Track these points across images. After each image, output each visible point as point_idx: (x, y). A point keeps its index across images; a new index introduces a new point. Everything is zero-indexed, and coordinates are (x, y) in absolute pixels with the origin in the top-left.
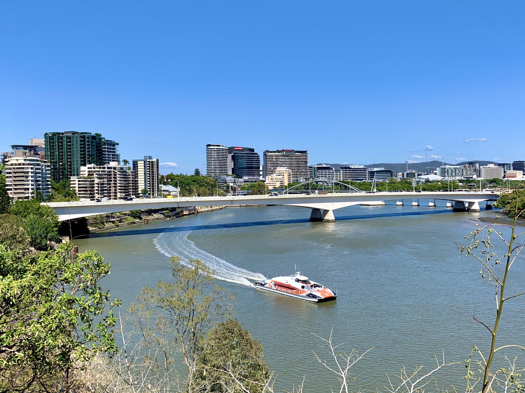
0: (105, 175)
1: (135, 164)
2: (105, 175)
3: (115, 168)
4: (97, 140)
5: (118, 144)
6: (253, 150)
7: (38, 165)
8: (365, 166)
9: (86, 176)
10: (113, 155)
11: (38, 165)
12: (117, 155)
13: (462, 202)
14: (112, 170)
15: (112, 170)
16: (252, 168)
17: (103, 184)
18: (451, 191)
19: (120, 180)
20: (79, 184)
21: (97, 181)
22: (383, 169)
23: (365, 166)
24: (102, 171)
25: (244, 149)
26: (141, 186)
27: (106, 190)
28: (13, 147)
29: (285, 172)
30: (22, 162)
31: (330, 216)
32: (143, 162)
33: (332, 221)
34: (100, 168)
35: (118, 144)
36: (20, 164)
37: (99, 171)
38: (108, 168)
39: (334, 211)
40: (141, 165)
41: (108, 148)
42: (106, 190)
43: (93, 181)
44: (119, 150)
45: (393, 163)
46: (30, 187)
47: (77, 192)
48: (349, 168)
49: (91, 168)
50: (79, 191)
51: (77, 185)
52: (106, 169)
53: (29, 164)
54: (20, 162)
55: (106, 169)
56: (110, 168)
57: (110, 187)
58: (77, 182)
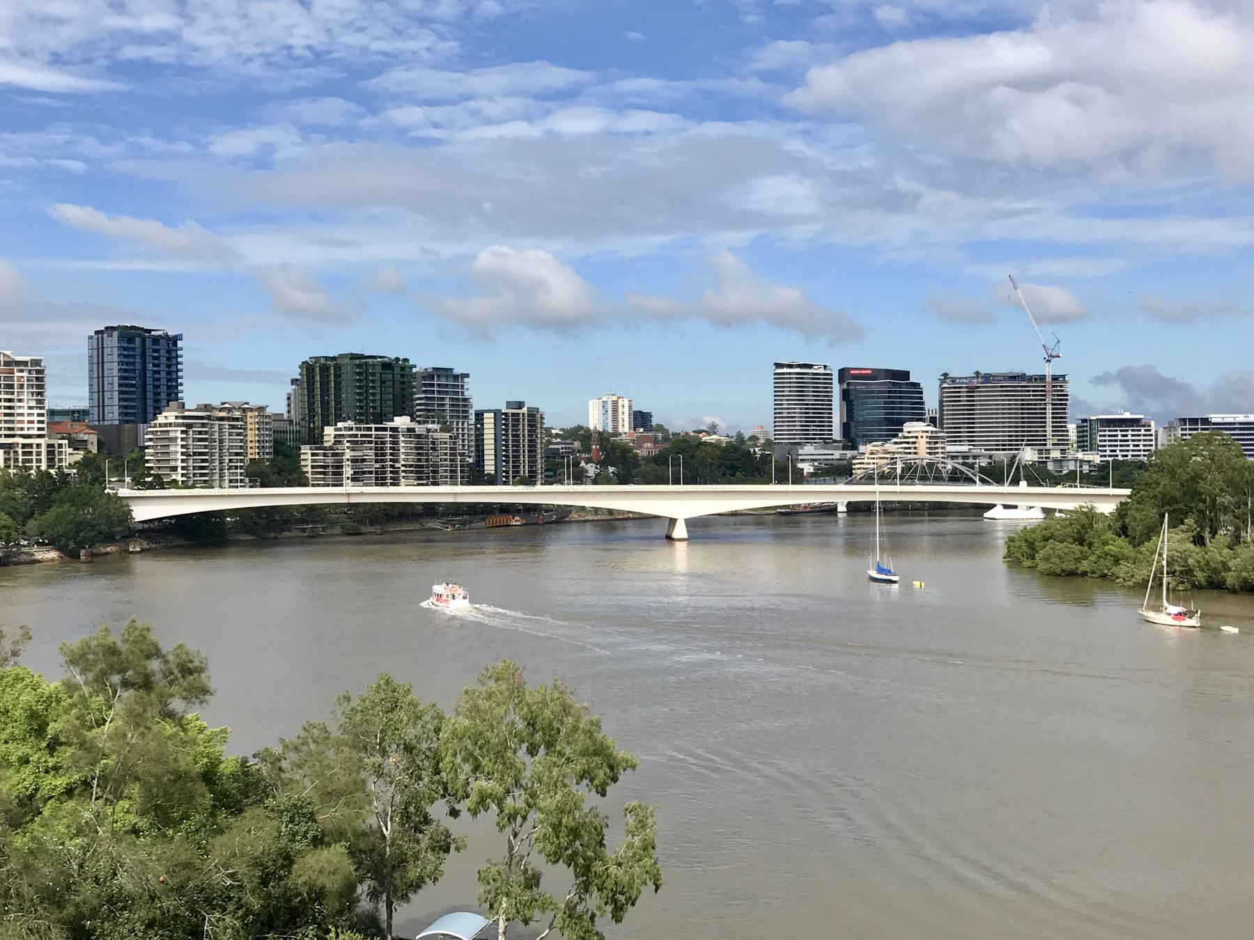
0: (370, 442)
1: (479, 416)
2: (370, 442)
3: (394, 430)
4: (397, 370)
5: (467, 376)
6: (906, 375)
7: (203, 425)
11: (203, 425)
12: (465, 400)
17: (364, 460)
18: (505, 483)
19: (407, 454)
20: (313, 461)
21: (348, 454)
24: (362, 436)
25: (876, 374)
26: (489, 467)
27: (371, 472)
29: (919, 435)
30: (172, 420)
31: (680, 531)
32: (492, 415)
34: (358, 429)
35: (467, 376)
36: (166, 425)
37: (356, 436)
39: (691, 523)
40: (489, 419)
41: (439, 385)
42: (371, 472)
46: (179, 464)
47: (309, 475)
48: (1206, 421)
49: (340, 429)
50: (313, 473)
51: (309, 463)
55: (373, 432)
56: (385, 429)
57: (383, 467)
58: (309, 457)
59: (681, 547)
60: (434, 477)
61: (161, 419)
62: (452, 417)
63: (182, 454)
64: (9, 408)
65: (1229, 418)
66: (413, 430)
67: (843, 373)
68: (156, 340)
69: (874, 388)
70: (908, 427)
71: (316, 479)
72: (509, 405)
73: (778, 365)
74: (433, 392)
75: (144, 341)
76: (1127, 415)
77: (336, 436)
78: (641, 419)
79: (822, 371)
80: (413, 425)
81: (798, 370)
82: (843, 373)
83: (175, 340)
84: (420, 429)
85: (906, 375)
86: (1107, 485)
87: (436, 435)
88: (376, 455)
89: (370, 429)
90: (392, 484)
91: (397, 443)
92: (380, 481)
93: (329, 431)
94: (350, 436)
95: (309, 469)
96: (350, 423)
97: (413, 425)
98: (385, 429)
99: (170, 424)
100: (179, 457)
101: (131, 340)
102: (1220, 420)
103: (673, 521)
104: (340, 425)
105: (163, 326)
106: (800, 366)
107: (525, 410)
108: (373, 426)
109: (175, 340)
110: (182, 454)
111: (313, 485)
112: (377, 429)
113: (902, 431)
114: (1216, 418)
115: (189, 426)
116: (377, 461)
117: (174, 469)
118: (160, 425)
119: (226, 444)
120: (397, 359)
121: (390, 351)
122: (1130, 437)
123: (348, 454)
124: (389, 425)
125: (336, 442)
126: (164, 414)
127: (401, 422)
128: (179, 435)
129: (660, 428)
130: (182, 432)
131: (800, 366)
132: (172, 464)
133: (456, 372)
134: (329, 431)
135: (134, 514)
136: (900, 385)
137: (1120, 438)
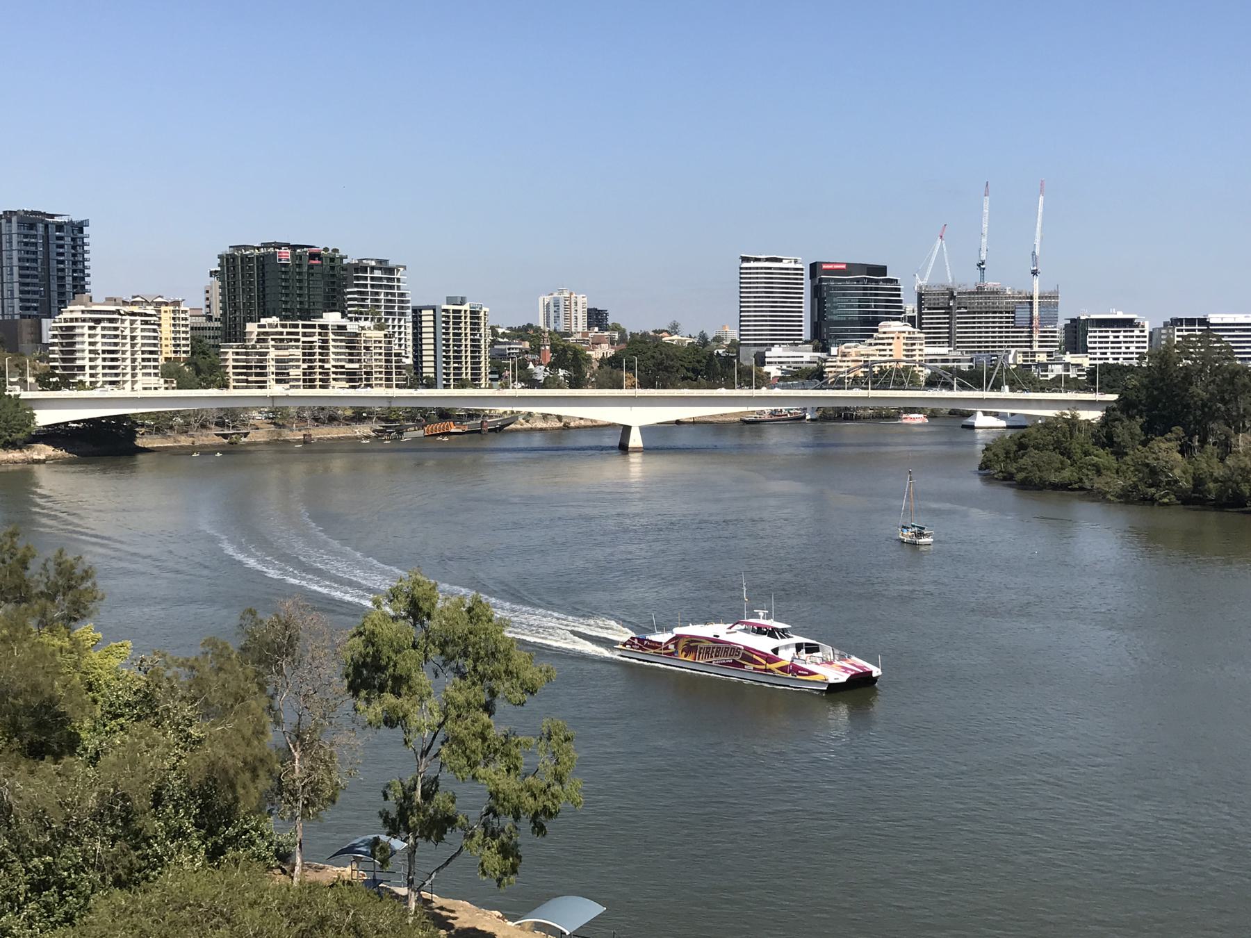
1: (417, 312)
2: (298, 340)
6: (882, 270)
7: (111, 320)
10: (387, 294)
11: (111, 320)
12: (402, 295)
14: (317, 330)
15: (317, 330)
18: (446, 386)
21: (273, 353)
24: (288, 333)
25: (851, 268)
26: (428, 370)
30: (79, 315)
31: (635, 440)
32: (431, 312)
33: (636, 450)
34: (284, 326)
36: (72, 320)
37: (282, 333)
38: (321, 326)
39: (644, 430)
40: (427, 316)
41: (373, 279)
43: (266, 354)
46: (87, 363)
48: (1203, 322)
49: (264, 326)
52: (300, 330)
53: (84, 320)
55: (300, 330)
56: (313, 326)
59: (635, 459)
60: (367, 379)
61: (66, 315)
62: (387, 313)
63: (91, 352)
64: (112, 360)
65: (1229, 318)
66: (344, 327)
68: (60, 227)
69: (848, 284)
70: (884, 326)
71: (238, 381)
72: (450, 300)
73: (745, 259)
74: (365, 286)
75: (46, 226)
77: (259, 334)
78: (596, 317)
79: (792, 265)
80: (344, 322)
81: (466, 342)
82: (814, 267)
83: (80, 227)
84: (352, 327)
87: (369, 333)
88: (304, 354)
89: (296, 326)
90: (321, 387)
91: (326, 341)
92: (309, 383)
93: (251, 327)
94: (277, 333)
96: (275, 320)
97: (344, 322)
98: (313, 326)
99: (77, 320)
100: (87, 355)
101: (32, 226)
102: (1219, 321)
103: (627, 430)
104: (263, 321)
105: (64, 208)
106: (767, 260)
107: (466, 307)
108: (300, 323)
109: (80, 227)
110: (91, 352)
111: (235, 387)
112: (304, 326)
113: (876, 331)
114: (1214, 319)
115: (98, 321)
116: (304, 361)
117: (82, 368)
118: (65, 320)
119: (139, 341)
120: (326, 249)
121: (320, 242)
122: (1121, 339)
124: (317, 322)
125: (258, 341)
126: (70, 308)
127: (332, 318)
128: (86, 331)
129: (616, 328)
131: (767, 260)
132: (79, 363)
133: (391, 264)
134: (251, 327)
135: (37, 418)
136: (877, 281)
137: (1111, 339)
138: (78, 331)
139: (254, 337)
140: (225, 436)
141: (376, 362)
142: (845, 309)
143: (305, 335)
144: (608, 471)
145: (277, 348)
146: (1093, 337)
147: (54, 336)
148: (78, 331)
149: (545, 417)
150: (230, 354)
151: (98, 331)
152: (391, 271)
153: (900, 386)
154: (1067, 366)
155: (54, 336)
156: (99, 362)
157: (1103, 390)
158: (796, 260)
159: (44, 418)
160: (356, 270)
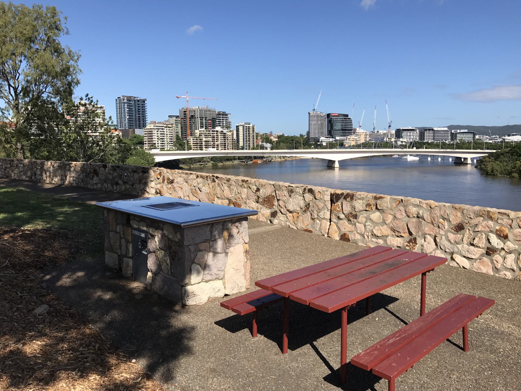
1: (237, 127)
3: (217, 131)
6: (347, 116)
7: (163, 129)
8: (448, 127)
9: (198, 136)
11: (163, 129)
13: (461, 158)
16: (346, 130)
21: (204, 139)
22: (466, 131)
23: (448, 127)
25: (339, 115)
26: (241, 144)
28: (169, 116)
30: (153, 127)
31: (337, 165)
36: (151, 129)
39: (339, 162)
40: (241, 128)
44: (230, 118)
45: (511, 124)
46: (156, 142)
48: (432, 130)
52: (211, 132)
54: (151, 127)
55: (211, 132)
56: (214, 131)
58: (192, 140)
65: (439, 129)
67: (328, 115)
68: (138, 101)
72: (246, 124)
76: (410, 128)
85: (347, 116)
86: (471, 149)
95: (192, 144)
99: (153, 129)
100: (156, 140)
105: (140, 96)
114: (435, 129)
115: (158, 129)
119: (168, 136)
123: (204, 139)
128: (156, 132)
130: (157, 131)
132: (154, 142)
133: (227, 113)
138: (153, 132)
139: (198, 134)
140: (201, 165)
141: (229, 142)
142: (338, 126)
143: (212, 134)
144: (328, 174)
145: (206, 138)
146: (404, 134)
147: (145, 134)
148: (153, 132)
149: (280, 157)
150: (191, 140)
151: (159, 132)
152: (227, 115)
153: (392, 147)
154: (402, 142)
155: (145, 134)
156: (159, 142)
157: (488, 149)
158: (325, 114)
159: (158, 159)
160: (218, 115)
